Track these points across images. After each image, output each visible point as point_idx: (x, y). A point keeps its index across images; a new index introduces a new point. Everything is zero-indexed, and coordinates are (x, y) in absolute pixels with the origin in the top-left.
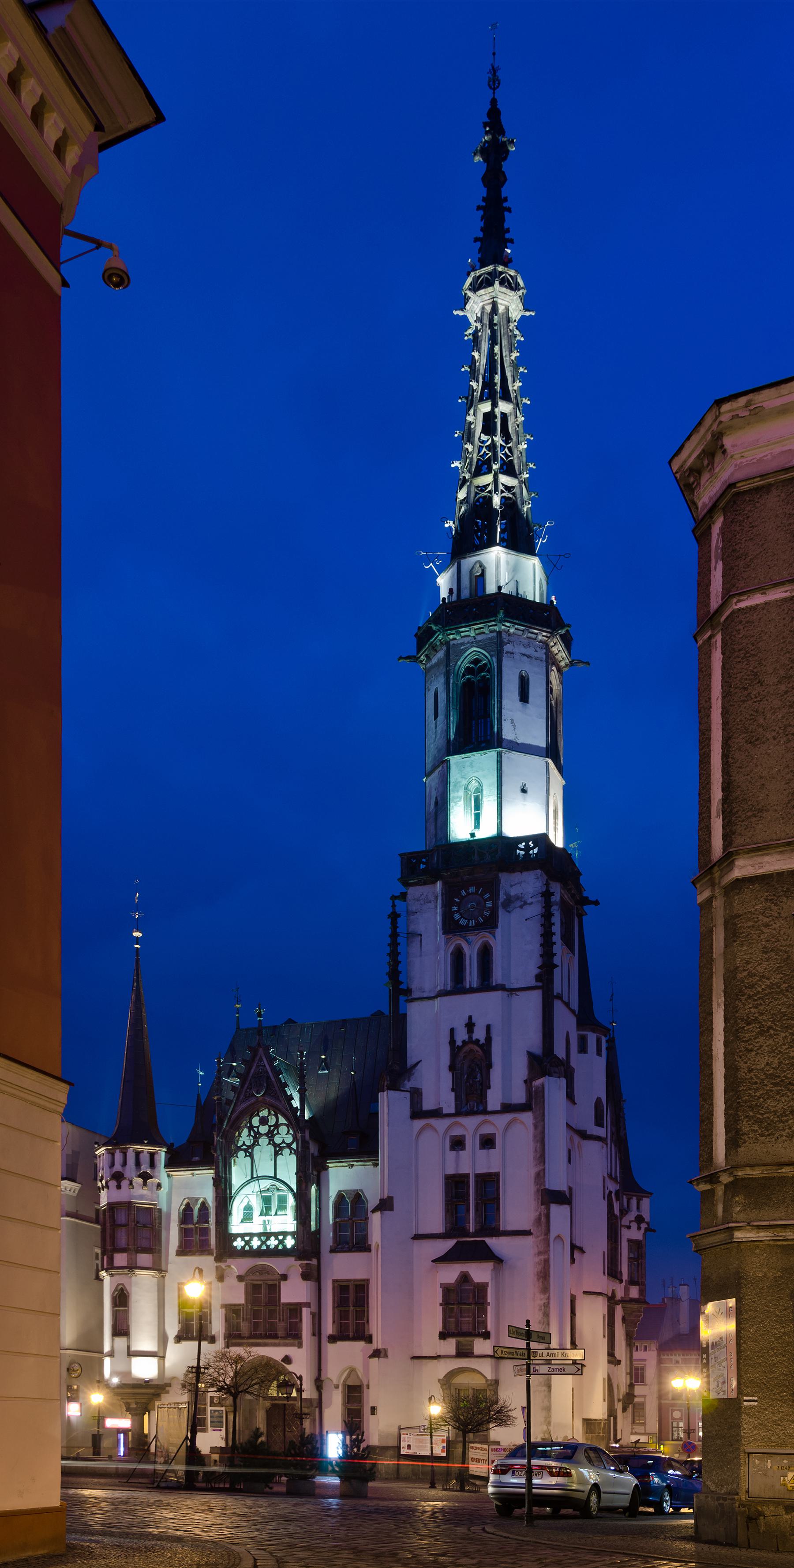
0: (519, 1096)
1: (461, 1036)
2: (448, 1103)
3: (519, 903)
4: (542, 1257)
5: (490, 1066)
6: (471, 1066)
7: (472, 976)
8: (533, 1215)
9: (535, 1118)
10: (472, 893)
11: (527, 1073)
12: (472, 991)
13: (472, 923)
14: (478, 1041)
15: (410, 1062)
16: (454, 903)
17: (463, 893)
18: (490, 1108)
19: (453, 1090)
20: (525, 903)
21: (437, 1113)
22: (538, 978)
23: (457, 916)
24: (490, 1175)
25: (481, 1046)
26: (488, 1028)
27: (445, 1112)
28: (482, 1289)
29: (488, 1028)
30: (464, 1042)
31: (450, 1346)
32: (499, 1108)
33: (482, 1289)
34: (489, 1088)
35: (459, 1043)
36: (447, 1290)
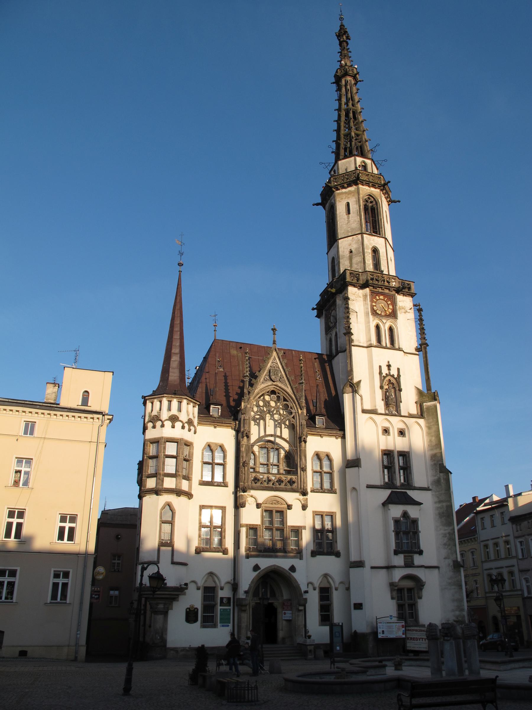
0: (414, 410)
1: (385, 371)
2: (381, 407)
3: (403, 311)
4: (444, 504)
5: (400, 390)
6: (392, 389)
7: (386, 340)
8: (431, 479)
9: (427, 422)
11: (417, 398)
12: (386, 348)
13: (383, 314)
14: (393, 376)
15: (355, 380)
17: (377, 297)
18: (403, 414)
19: (383, 400)
20: (407, 312)
21: (374, 412)
22: (418, 350)
24: (404, 452)
25: (396, 379)
26: (398, 369)
27: (379, 412)
28: (415, 522)
29: (398, 369)
30: (386, 374)
31: (399, 560)
32: (407, 415)
33: (415, 522)
34: (401, 402)
35: (384, 374)
36: (397, 522)
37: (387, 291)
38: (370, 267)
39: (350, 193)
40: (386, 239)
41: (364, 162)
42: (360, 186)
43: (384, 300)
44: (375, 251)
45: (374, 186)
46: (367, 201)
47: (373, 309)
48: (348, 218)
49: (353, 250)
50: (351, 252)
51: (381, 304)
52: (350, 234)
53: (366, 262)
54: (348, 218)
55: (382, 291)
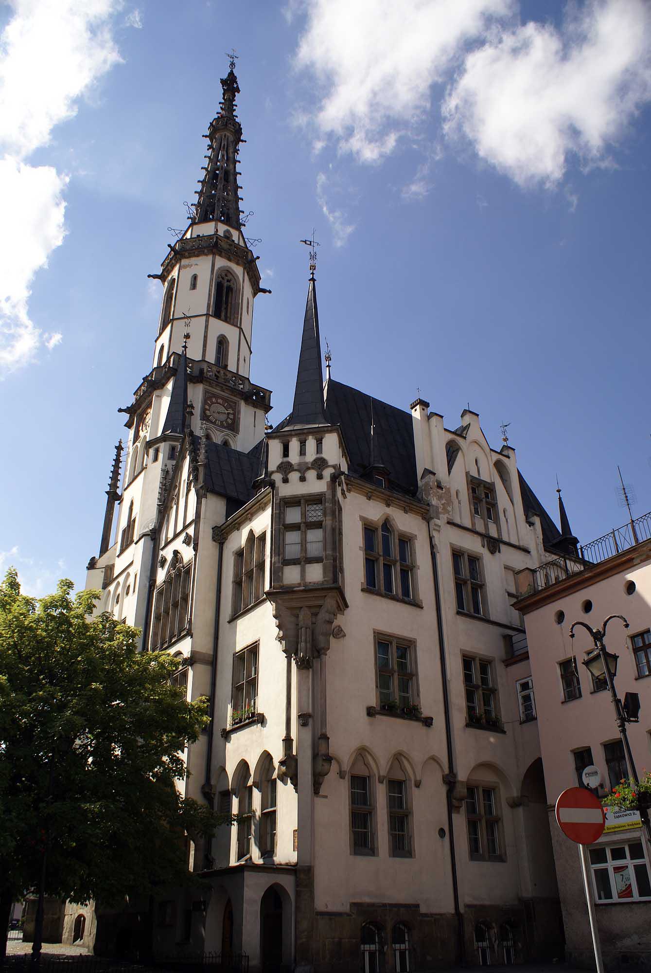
23: (208, 413)
38: (211, 357)
44: (222, 342)
47: (204, 413)
51: (218, 410)
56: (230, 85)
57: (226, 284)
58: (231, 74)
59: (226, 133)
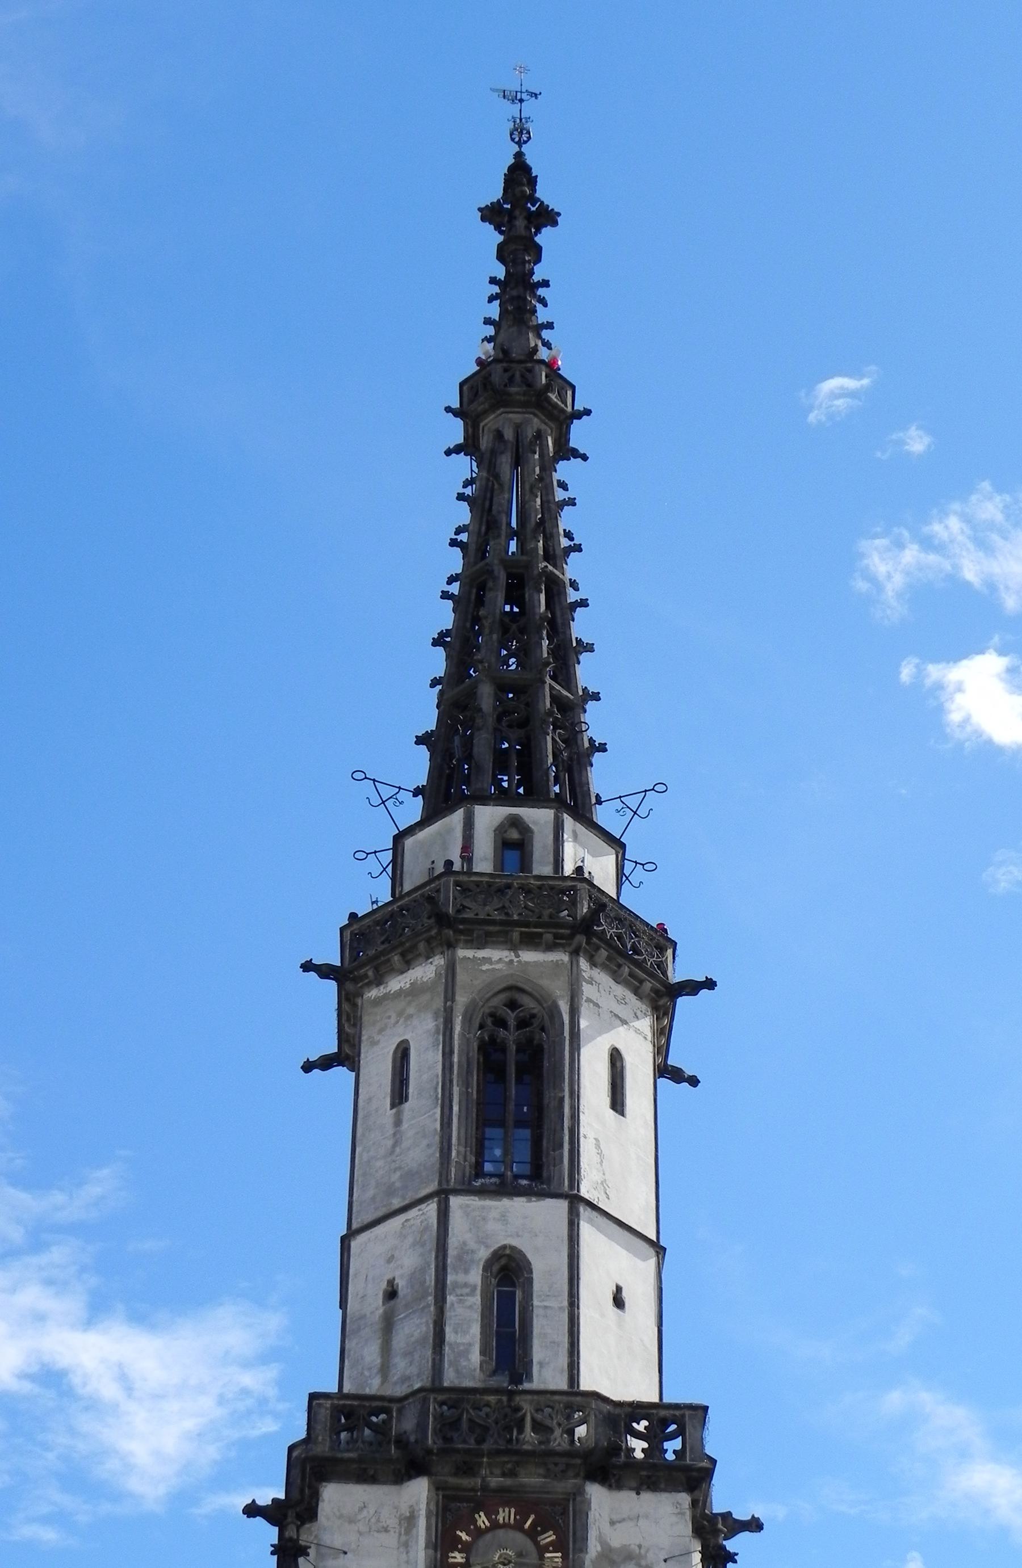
10: (505, 1526)
16: (454, 1543)
17: (482, 1520)
37: (531, 1479)
39: (415, 991)
40: (576, 1201)
41: (515, 822)
42: (462, 953)
43: (518, 1526)
44: (509, 1271)
45: (531, 941)
46: (500, 1022)
48: (398, 1122)
49: (401, 1283)
50: (391, 1294)
52: (397, 1203)
53: (450, 1336)
54: (398, 1122)
55: (508, 1482)
56: (519, 214)
57: (510, 1037)
58: (519, 175)
59: (515, 408)
